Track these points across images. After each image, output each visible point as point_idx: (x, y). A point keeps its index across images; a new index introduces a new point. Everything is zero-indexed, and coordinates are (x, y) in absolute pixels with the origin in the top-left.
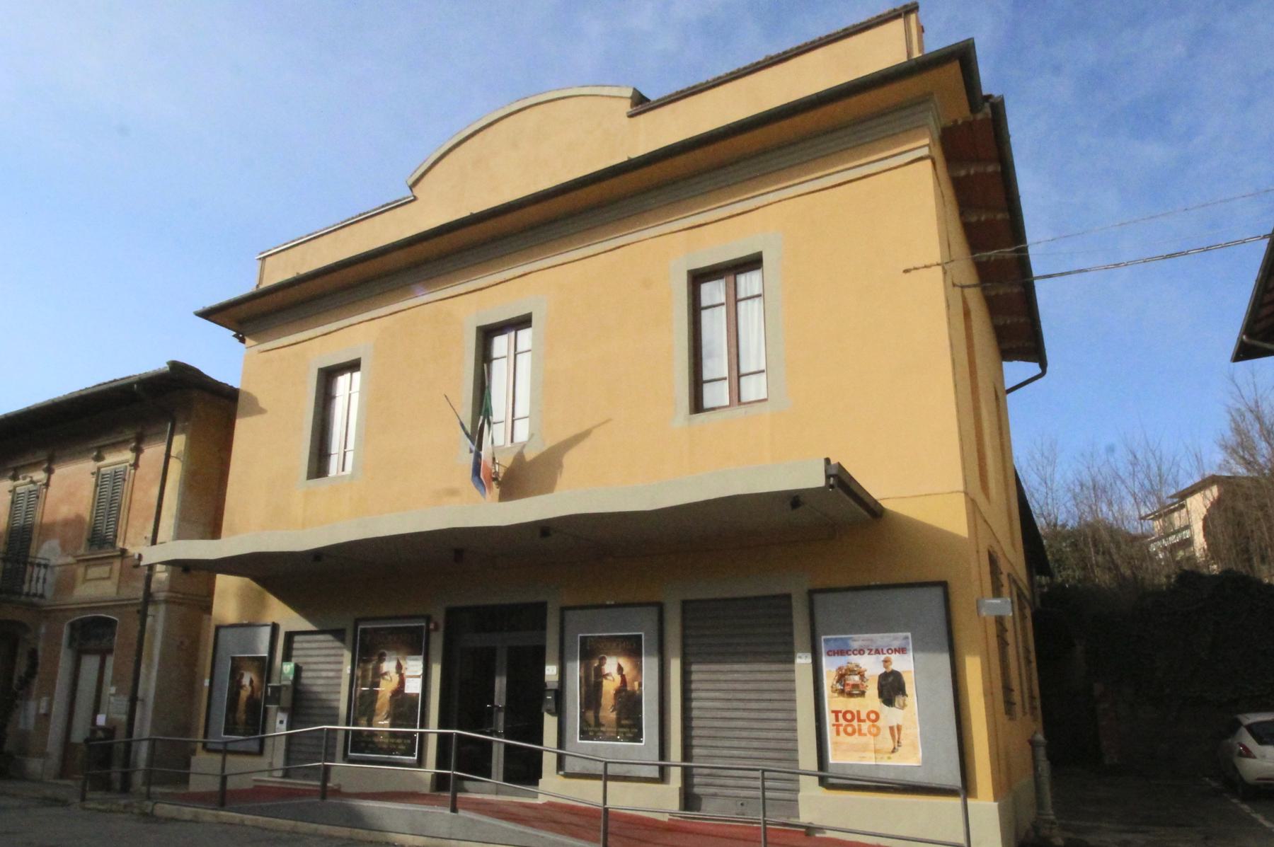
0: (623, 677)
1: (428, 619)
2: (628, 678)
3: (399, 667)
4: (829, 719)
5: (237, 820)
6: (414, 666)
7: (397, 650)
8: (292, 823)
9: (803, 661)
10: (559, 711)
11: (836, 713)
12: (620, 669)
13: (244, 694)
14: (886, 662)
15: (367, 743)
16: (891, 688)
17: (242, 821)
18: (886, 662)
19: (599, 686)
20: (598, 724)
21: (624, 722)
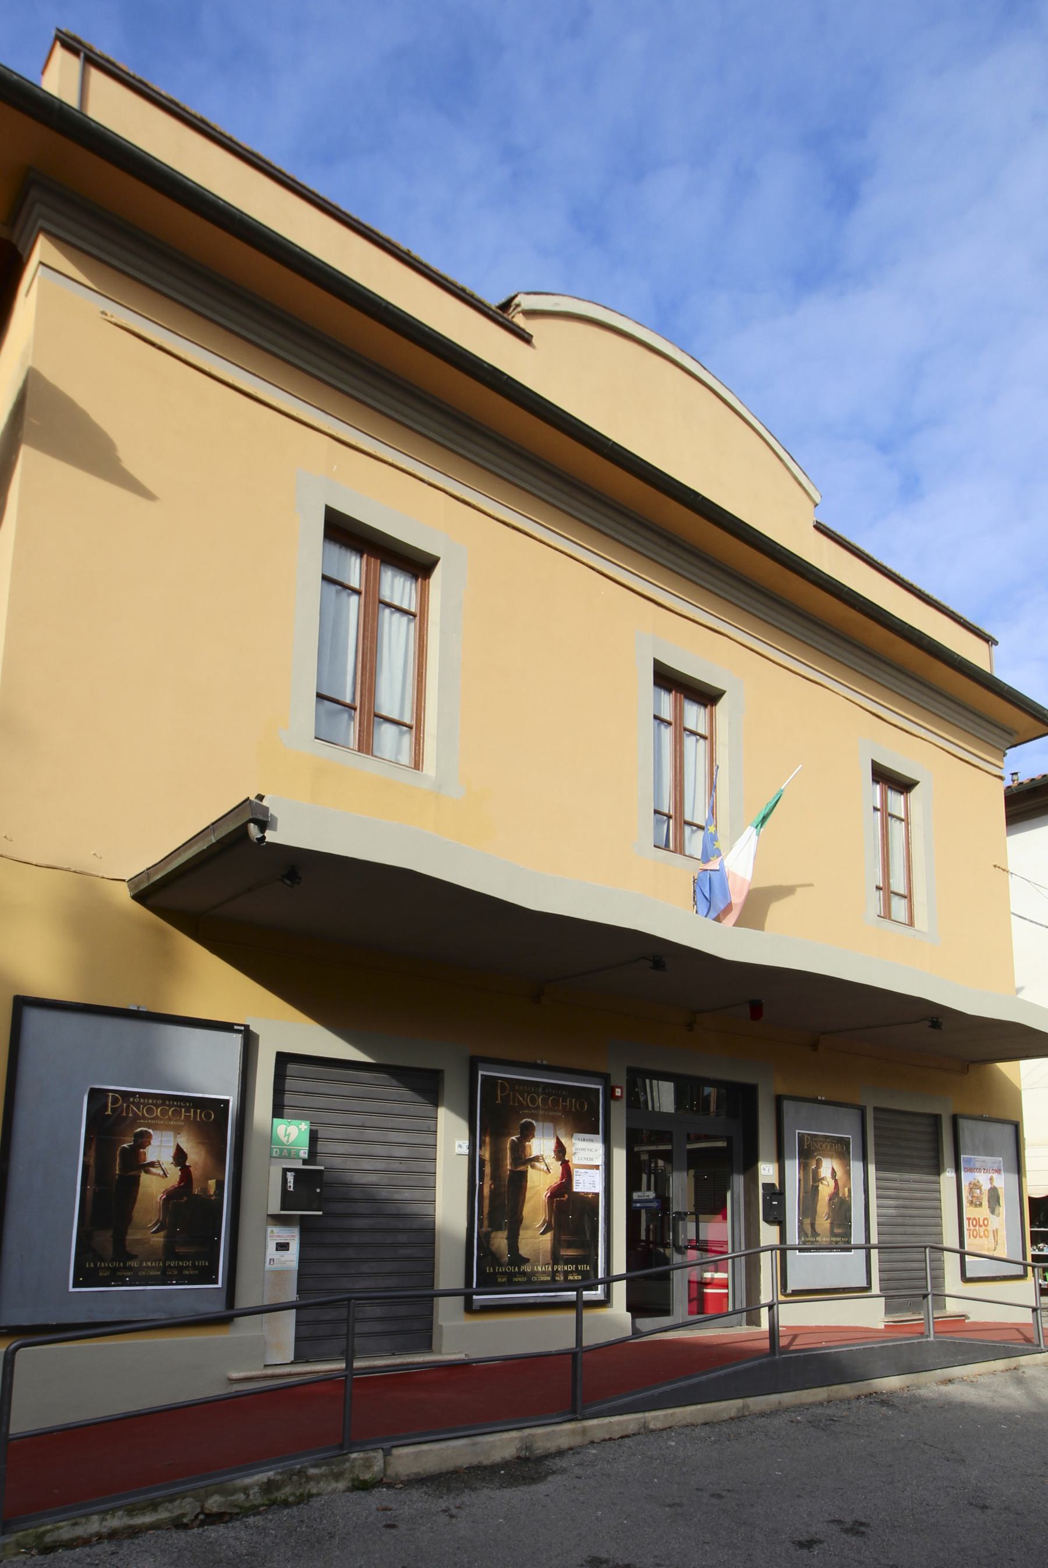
0: (186, 1172)
1: (605, 1078)
2: (196, 1173)
3: (560, 1151)
4: (966, 1222)
5: (632, 1428)
6: (586, 1151)
7: (554, 1120)
8: (739, 1403)
9: (948, 1177)
10: (777, 1219)
11: (969, 1219)
12: (180, 1156)
13: (154, 1187)
14: (991, 1179)
15: (511, 1275)
16: (994, 1197)
17: (645, 1425)
18: (991, 1179)
19: (815, 1190)
20: (122, 1252)
21: (837, 1231)
